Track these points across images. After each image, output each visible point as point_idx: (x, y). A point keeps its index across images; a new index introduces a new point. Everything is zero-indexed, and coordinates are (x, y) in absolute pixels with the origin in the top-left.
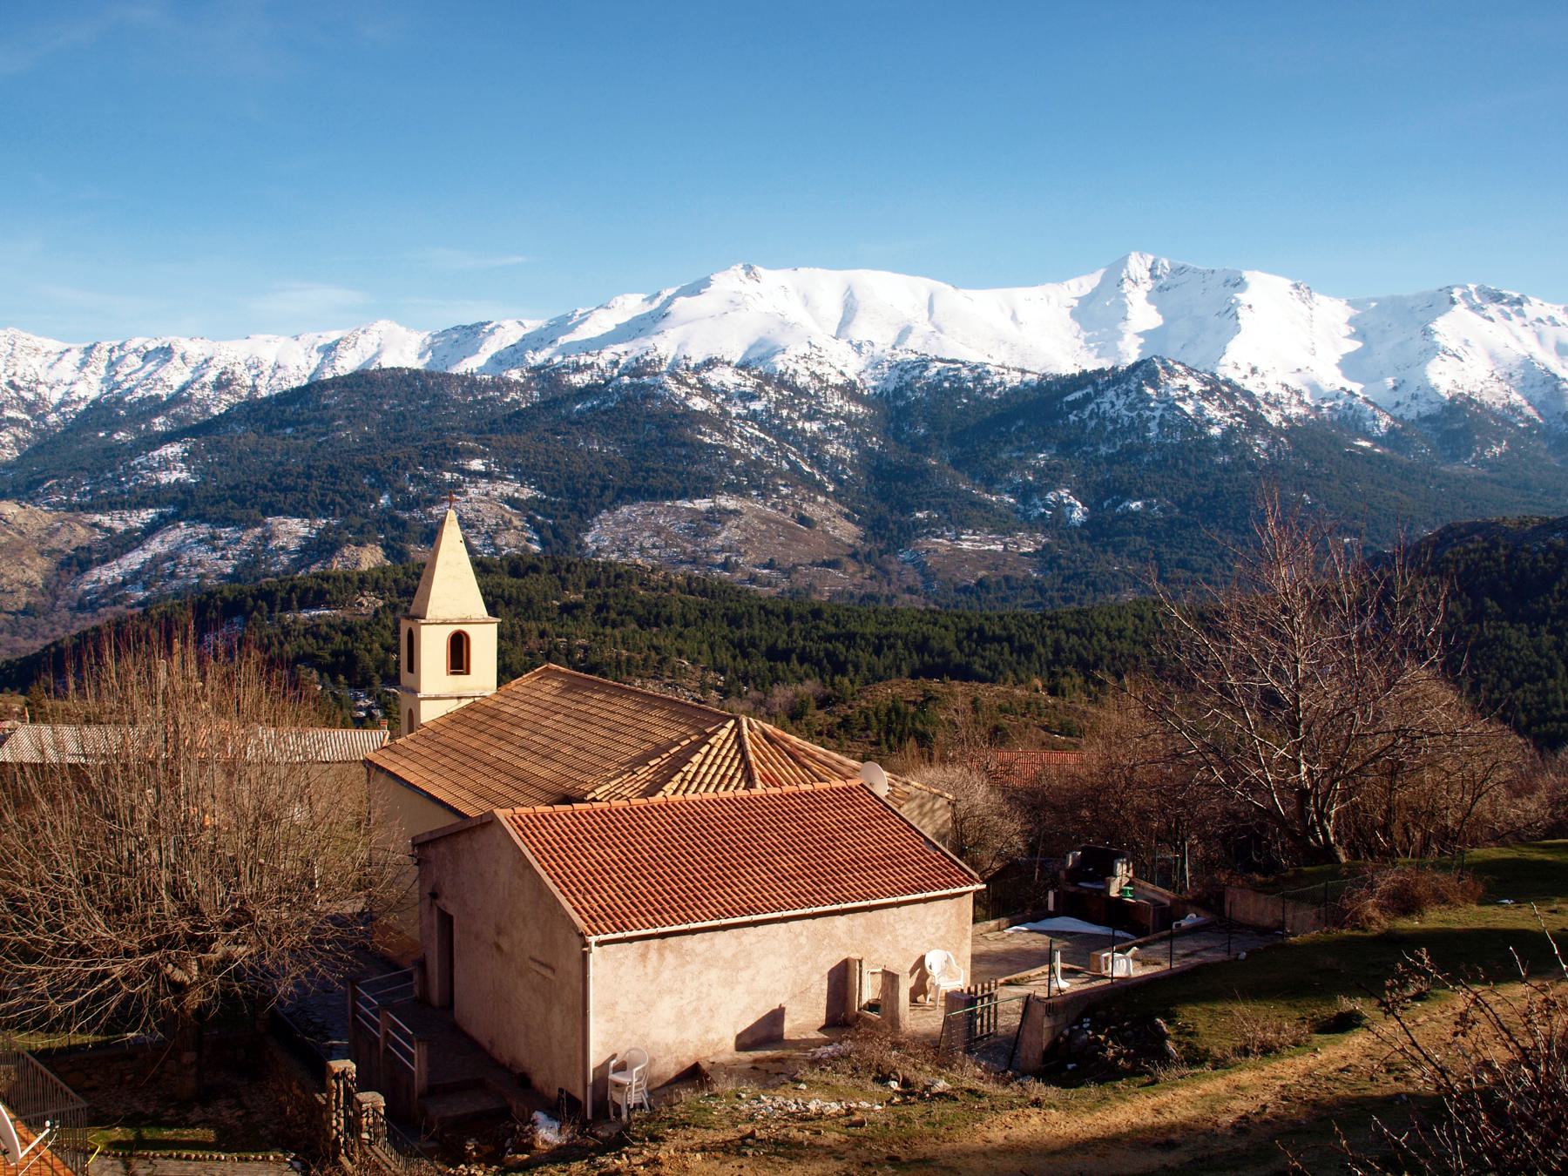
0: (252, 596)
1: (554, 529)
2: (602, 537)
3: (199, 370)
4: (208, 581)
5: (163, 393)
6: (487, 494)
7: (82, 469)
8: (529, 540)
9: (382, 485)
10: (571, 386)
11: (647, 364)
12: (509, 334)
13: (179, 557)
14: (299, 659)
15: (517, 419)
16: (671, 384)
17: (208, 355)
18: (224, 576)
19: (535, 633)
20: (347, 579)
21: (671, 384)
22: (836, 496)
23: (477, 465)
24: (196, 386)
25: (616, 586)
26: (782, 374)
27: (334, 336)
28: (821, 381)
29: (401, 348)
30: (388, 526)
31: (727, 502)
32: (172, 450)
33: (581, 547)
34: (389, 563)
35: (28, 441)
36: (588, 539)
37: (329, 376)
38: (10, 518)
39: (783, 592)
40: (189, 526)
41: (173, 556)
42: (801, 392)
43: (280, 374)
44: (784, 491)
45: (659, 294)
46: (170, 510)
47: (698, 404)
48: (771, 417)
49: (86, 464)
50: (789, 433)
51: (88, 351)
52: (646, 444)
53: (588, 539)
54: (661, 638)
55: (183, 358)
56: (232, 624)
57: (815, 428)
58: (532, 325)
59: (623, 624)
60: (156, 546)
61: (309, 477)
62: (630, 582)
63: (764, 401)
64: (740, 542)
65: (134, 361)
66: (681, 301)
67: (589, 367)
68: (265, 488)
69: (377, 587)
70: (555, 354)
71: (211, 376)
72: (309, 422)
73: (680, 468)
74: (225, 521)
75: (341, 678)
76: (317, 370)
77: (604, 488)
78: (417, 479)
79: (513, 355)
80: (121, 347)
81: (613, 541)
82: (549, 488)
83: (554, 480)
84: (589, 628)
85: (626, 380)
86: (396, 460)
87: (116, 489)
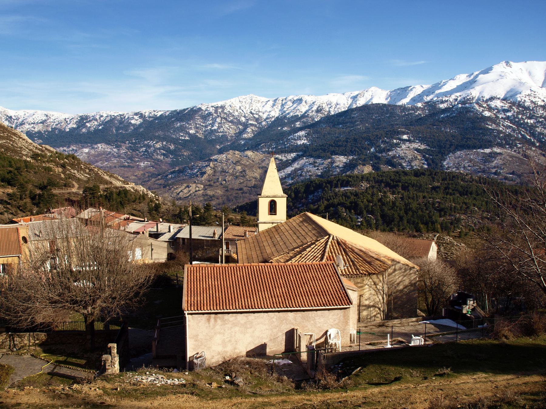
0: (325, 182)
1: (433, 160)
2: (449, 163)
3: (311, 106)
4: (313, 177)
5: (299, 114)
6: (409, 147)
7: (273, 140)
8: (423, 164)
9: (372, 144)
10: (440, 109)
11: (468, 100)
12: (418, 90)
13: (303, 169)
14: (339, 204)
15: (420, 120)
16: (477, 107)
17: (314, 101)
18: (318, 176)
19: (422, 197)
20: (357, 177)
21: (477, 107)
22: (539, 147)
23: (405, 137)
24: (310, 111)
25: (452, 180)
26: (519, 102)
27: (356, 93)
28: (535, 104)
29: (380, 97)
30: (374, 159)
31: (497, 150)
32: (302, 133)
33: (442, 166)
34: (374, 171)
35: (256, 131)
36: (445, 163)
37: (354, 107)
38: (250, 156)
39: (517, 183)
40: (307, 159)
41: (301, 169)
42: (527, 108)
43: (338, 106)
44: (519, 146)
45: (473, 74)
46: (300, 153)
47: (487, 114)
48: (515, 118)
49: (274, 138)
50: (522, 124)
51: (275, 101)
52: (467, 129)
53: (445, 163)
54: (467, 199)
55: (306, 102)
56: (318, 192)
57: (532, 121)
58: (426, 87)
59: (454, 194)
60: (296, 165)
61: (347, 142)
62: (458, 179)
63: (512, 112)
64: (501, 165)
65: (290, 104)
66: (481, 76)
67: (446, 101)
68: (332, 146)
69: (368, 180)
70: (434, 97)
71: (315, 108)
72: (347, 123)
73: (479, 137)
74: (319, 157)
75: (353, 211)
76: (350, 105)
77: (451, 145)
78: (384, 142)
79: (419, 98)
80: (286, 99)
81: (454, 164)
82: (431, 145)
83: (433, 142)
84: (441, 195)
85: (460, 106)
86: (377, 136)
87: (283, 147)
